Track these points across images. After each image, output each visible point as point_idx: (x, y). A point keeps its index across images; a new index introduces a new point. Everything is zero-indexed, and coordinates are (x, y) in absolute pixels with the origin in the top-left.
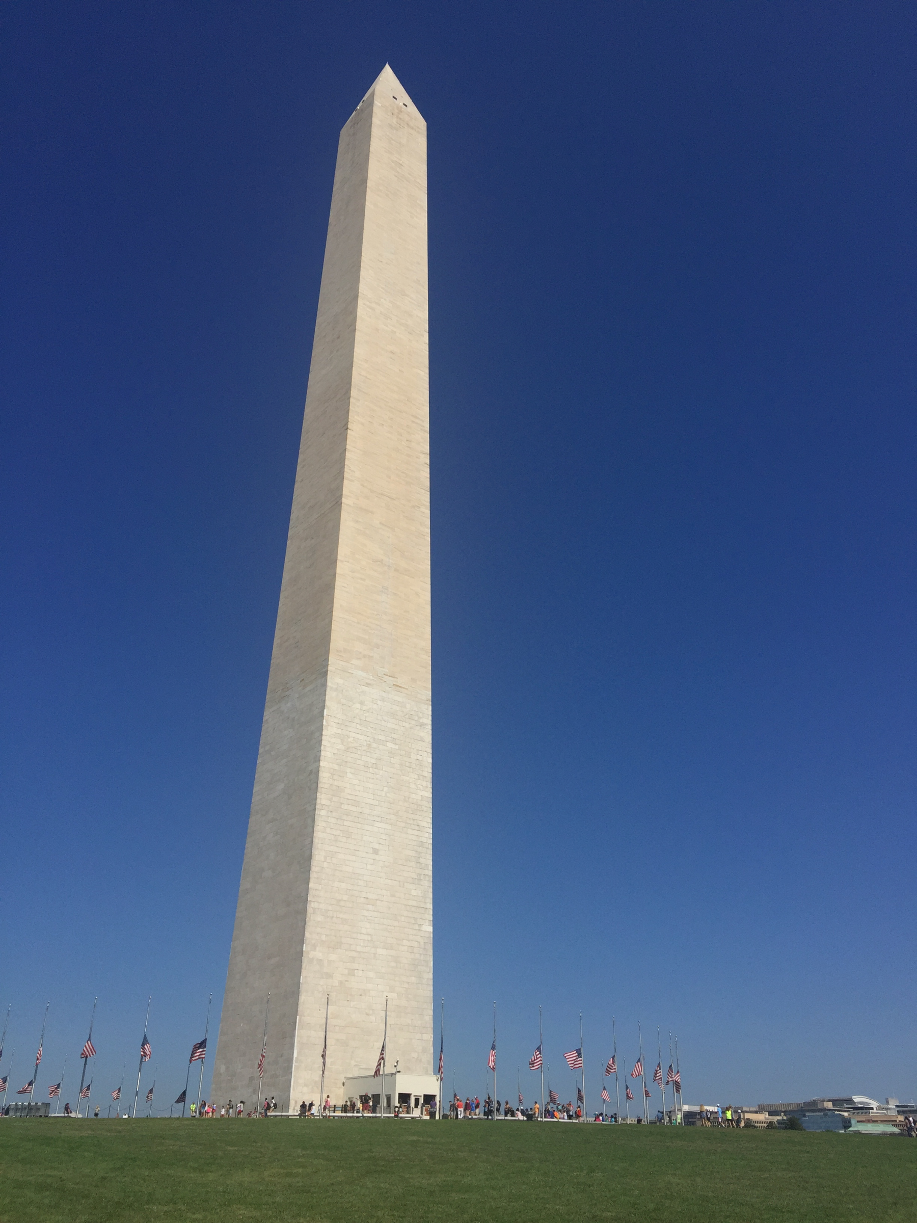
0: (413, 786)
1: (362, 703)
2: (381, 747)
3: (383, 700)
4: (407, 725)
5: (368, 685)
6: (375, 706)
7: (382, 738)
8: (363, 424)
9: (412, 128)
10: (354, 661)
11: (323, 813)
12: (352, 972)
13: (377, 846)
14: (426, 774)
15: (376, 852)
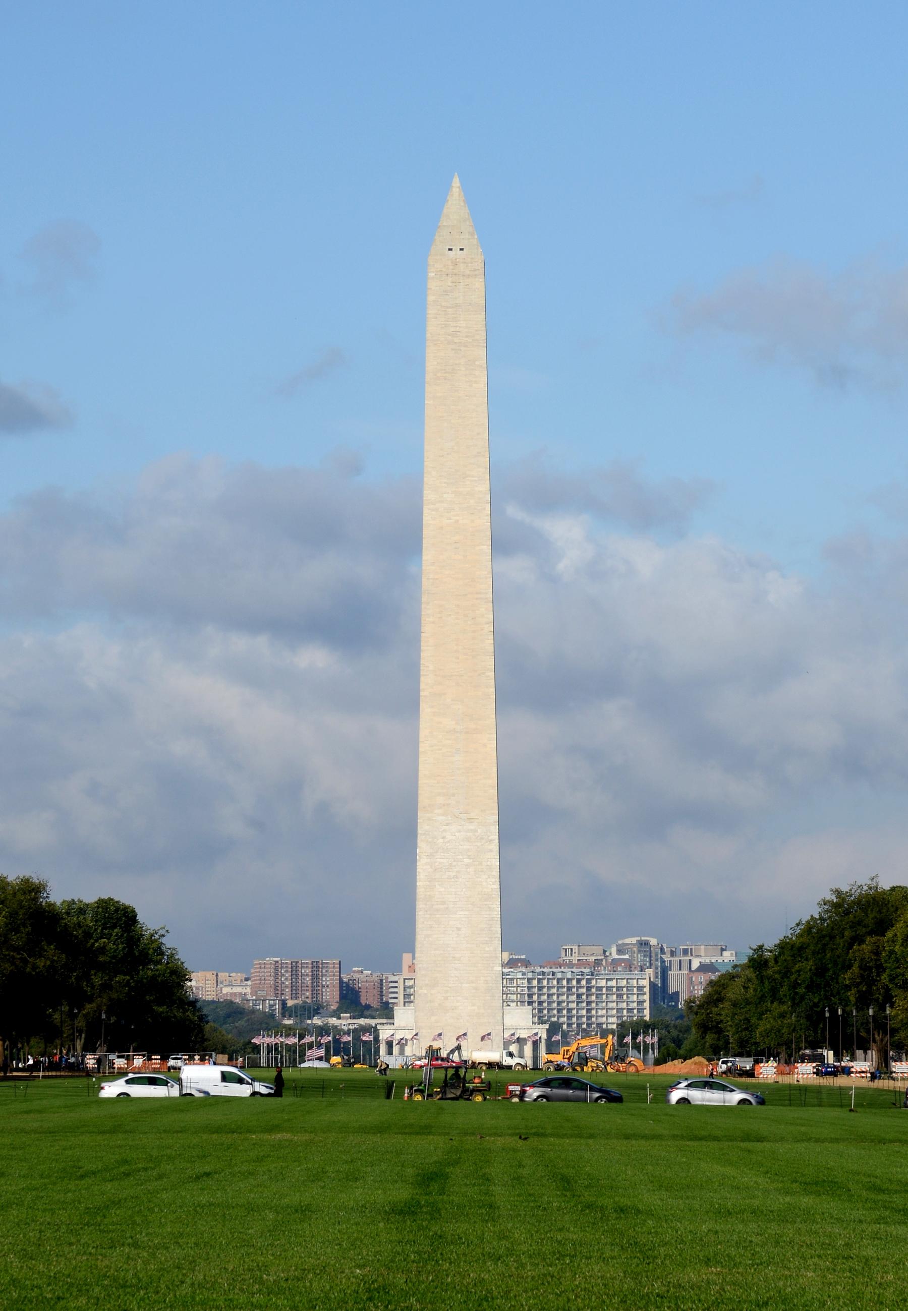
0: (484, 884)
1: (444, 838)
2: (460, 863)
3: (460, 831)
4: (479, 844)
5: (447, 824)
6: (454, 838)
7: (461, 857)
8: (433, 623)
9: (469, 276)
10: (436, 811)
11: (421, 913)
12: (446, 998)
13: (459, 926)
14: (494, 873)
15: (459, 929)
